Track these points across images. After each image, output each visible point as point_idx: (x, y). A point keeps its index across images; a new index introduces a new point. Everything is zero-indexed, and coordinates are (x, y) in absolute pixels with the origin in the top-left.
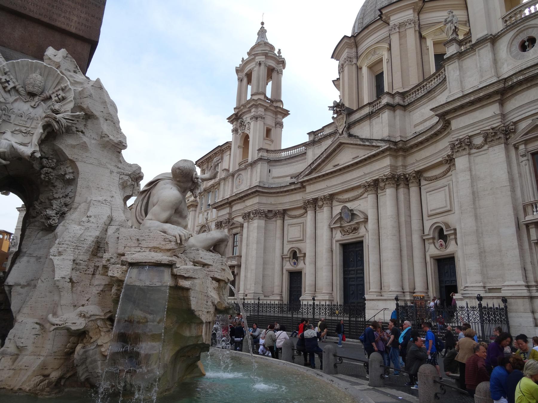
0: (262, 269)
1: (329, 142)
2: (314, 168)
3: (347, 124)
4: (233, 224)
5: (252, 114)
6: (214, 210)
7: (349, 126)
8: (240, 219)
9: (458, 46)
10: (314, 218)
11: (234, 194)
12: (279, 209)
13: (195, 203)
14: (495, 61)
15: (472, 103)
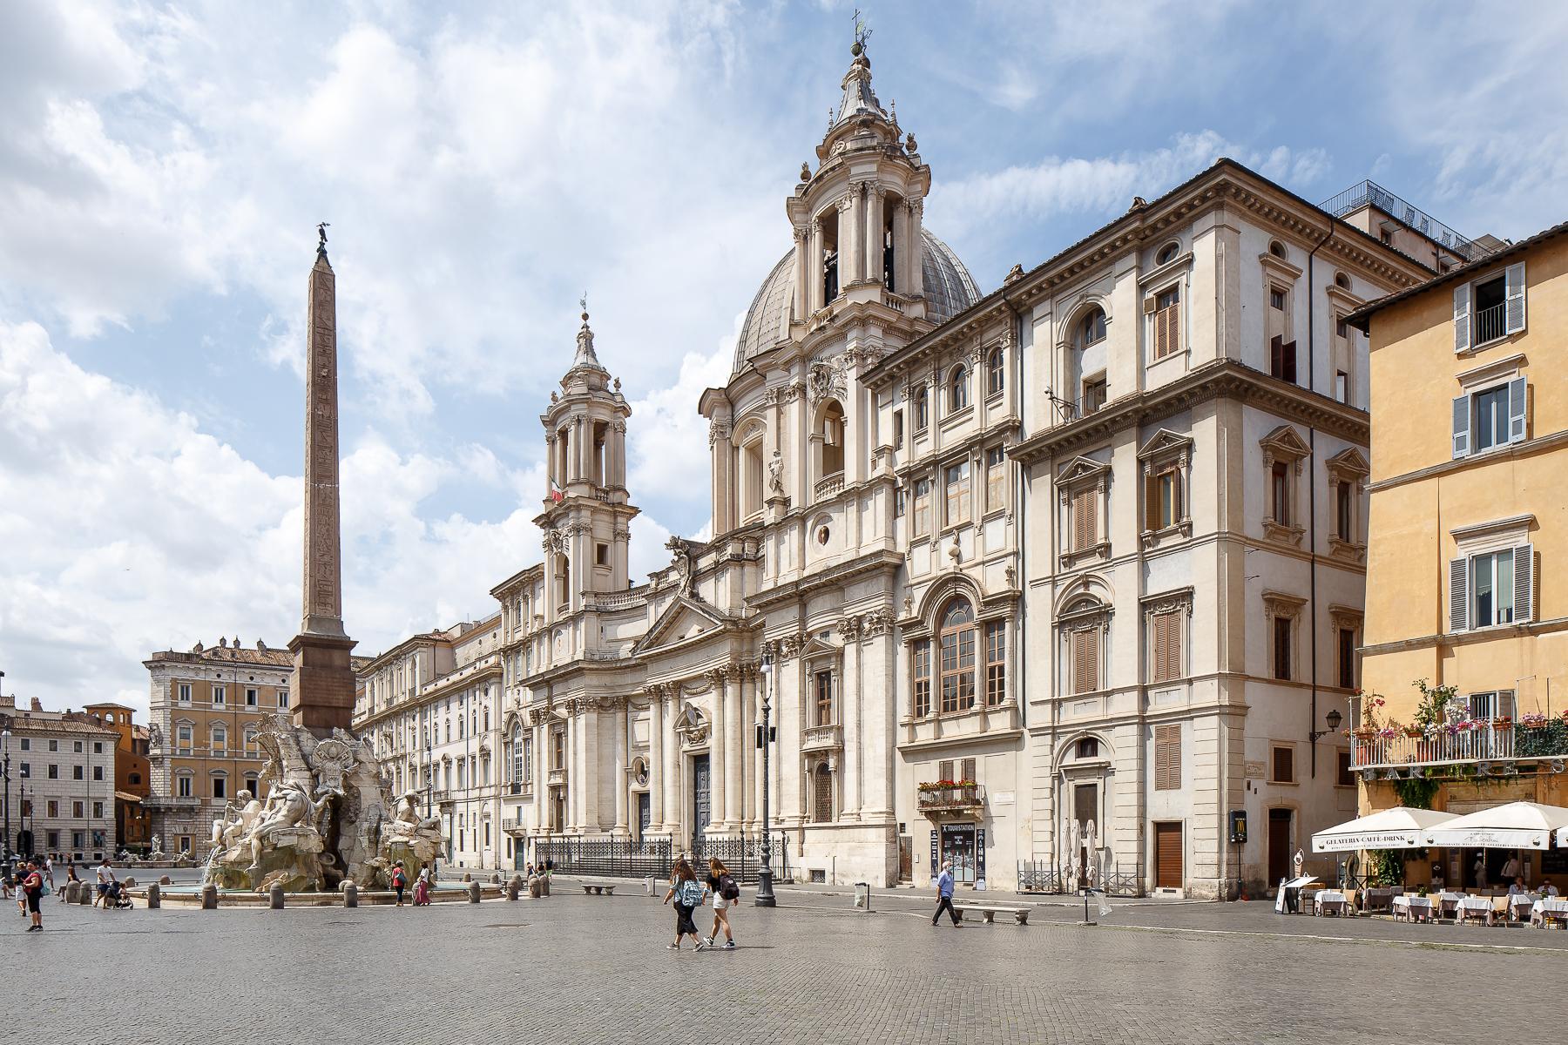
0: (596, 791)
1: (669, 601)
2: (655, 637)
3: (691, 573)
4: (554, 717)
5: (571, 522)
6: (527, 688)
7: (696, 578)
8: (562, 712)
9: (781, 507)
10: (659, 714)
11: (552, 668)
12: (618, 694)
13: (497, 670)
14: (803, 548)
15: (779, 600)
